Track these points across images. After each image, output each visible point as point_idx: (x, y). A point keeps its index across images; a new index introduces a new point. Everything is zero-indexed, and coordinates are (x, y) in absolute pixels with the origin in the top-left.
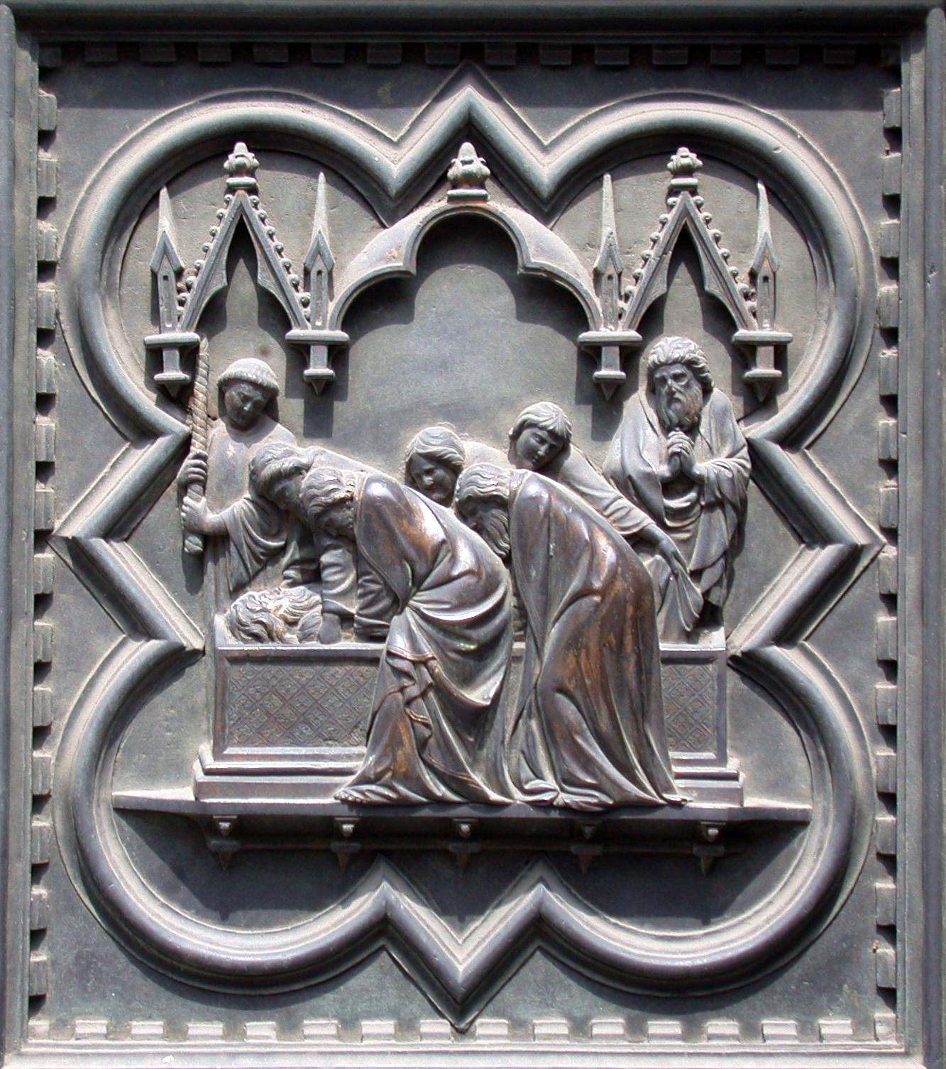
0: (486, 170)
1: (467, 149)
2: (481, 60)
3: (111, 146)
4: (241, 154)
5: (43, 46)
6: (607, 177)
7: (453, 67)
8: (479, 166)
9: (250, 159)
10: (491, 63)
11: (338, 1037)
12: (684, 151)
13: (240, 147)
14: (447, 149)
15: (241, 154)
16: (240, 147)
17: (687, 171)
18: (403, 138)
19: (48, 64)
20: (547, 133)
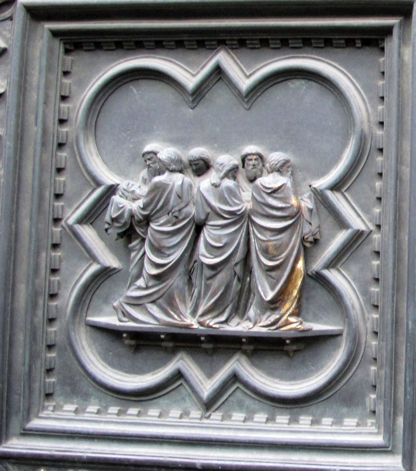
11: (288, 424)
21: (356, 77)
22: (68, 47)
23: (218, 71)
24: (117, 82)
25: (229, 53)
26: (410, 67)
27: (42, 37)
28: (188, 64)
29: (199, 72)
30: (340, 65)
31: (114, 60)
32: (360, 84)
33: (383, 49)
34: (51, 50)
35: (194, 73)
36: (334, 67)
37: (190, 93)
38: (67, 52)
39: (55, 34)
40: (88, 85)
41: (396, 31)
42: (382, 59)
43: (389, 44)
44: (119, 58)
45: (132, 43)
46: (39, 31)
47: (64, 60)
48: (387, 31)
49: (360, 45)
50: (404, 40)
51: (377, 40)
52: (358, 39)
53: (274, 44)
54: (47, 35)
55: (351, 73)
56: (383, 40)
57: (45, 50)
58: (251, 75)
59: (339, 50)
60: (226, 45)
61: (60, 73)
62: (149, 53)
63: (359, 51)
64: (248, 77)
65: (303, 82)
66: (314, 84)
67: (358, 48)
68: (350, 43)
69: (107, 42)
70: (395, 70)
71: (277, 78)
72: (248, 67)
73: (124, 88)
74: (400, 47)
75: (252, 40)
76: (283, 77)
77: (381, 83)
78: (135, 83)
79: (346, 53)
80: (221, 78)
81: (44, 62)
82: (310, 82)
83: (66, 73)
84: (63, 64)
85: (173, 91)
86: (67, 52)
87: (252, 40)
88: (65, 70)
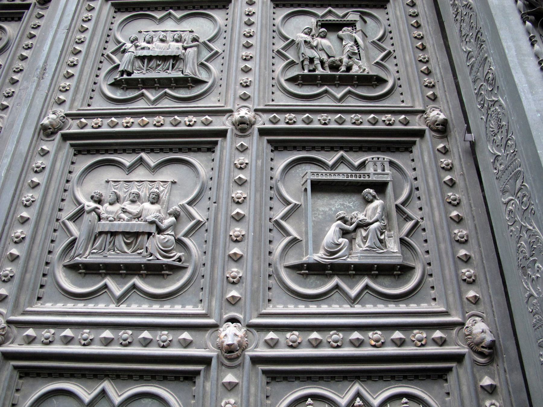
0: (363, 404)
1: (358, 399)
2: (359, 379)
3: (281, 399)
4: (309, 401)
5: (267, 377)
6: (388, 405)
7: (353, 381)
8: (361, 403)
9: (311, 402)
10: (361, 380)
12: (404, 399)
13: (309, 399)
14: (354, 399)
15: (309, 401)
16: (309, 399)
17: (406, 403)
18: (344, 397)
19: (268, 381)
20: (374, 395)
21: (179, 398)
22: (21, 375)
23: (103, 392)
24: (46, 396)
25: (110, 382)
26: (209, 393)
27: (8, 370)
28: (87, 387)
29: (92, 392)
30: (171, 390)
31: (46, 383)
32: (181, 402)
33: (195, 382)
34: (11, 377)
35: (90, 393)
36: (167, 391)
37: (86, 405)
38: (21, 377)
39: (15, 368)
40: (29, 397)
41: (202, 373)
42: (194, 388)
43: (198, 380)
44: (49, 382)
45: (58, 374)
46: (7, 366)
47: (18, 383)
48: (198, 373)
49: (182, 380)
50: (206, 378)
51: (192, 377)
52: (181, 377)
53: (135, 378)
54: (11, 368)
55: (176, 395)
56: (195, 377)
57: (8, 376)
58: (121, 395)
59: (171, 382)
60: (109, 377)
61: (14, 390)
62: (66, 380)
63: (182, 383)
64: (119, 396)
65: (150, 400)
66: (155, 401)
67: (182, 381)
68: (177, 379)
69: (43, 373)
70: (201, 395)
71: (135, 398)
72: (120, 391)
73: (49, 400)
74: (204, 382)
75: (124, 375)
76: (138, 397)
77: (193, 402)
78: (56, 397)
79: (174, 384)
80: (104, 396)
81: (6, 384)
82: (154, 400)
83: (18, 390)
84: (17, 385)
85: (77, 402)
86: (21, 377)
87: (124, 375)
88: (18, 388)
